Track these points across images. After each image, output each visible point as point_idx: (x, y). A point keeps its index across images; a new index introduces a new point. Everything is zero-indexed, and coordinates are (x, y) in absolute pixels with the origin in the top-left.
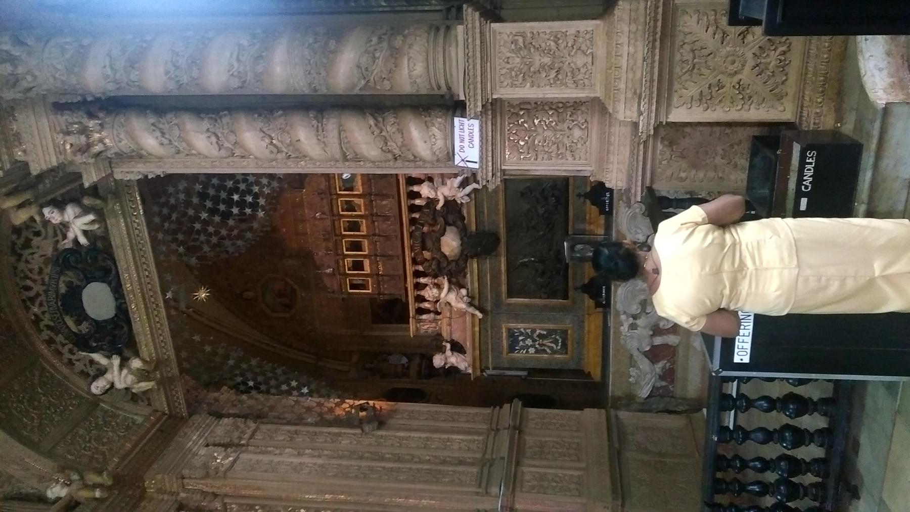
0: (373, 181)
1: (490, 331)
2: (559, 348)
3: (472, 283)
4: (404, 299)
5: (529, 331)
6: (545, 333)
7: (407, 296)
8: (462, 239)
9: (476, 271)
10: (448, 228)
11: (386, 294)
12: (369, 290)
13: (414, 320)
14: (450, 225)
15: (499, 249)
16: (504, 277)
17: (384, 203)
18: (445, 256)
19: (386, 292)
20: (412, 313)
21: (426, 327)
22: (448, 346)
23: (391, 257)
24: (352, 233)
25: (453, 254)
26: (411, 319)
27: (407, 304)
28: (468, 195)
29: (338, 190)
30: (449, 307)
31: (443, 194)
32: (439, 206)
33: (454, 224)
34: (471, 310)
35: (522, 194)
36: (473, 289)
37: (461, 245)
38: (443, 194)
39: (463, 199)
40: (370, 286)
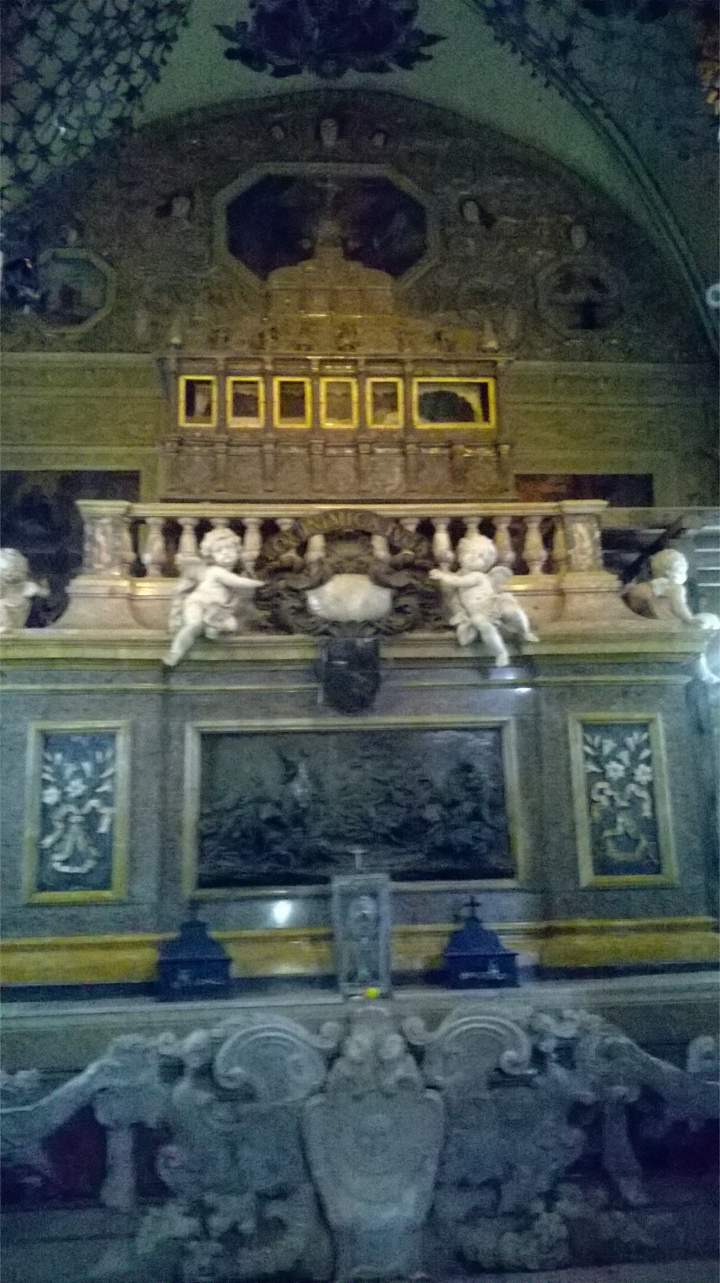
1: (108, 687)
2: (58, 866)
3: (251, 646)
5: (106, 787)
6: (103, 829)
8: (368, 624)
9: (280, 655)
13: (122, 510)
14: (394, 599)
15: (331, 712)
16: (258, 724)
20: (140, 509)
21: (100, 538)
22: (45, 592)
26: (126, 503)
28: (478, 641)
31: (476, 585)
32: (435, 574)
35: (467, 768)
36: (231, 647)
37: (352, 624)
38: (476, 585)
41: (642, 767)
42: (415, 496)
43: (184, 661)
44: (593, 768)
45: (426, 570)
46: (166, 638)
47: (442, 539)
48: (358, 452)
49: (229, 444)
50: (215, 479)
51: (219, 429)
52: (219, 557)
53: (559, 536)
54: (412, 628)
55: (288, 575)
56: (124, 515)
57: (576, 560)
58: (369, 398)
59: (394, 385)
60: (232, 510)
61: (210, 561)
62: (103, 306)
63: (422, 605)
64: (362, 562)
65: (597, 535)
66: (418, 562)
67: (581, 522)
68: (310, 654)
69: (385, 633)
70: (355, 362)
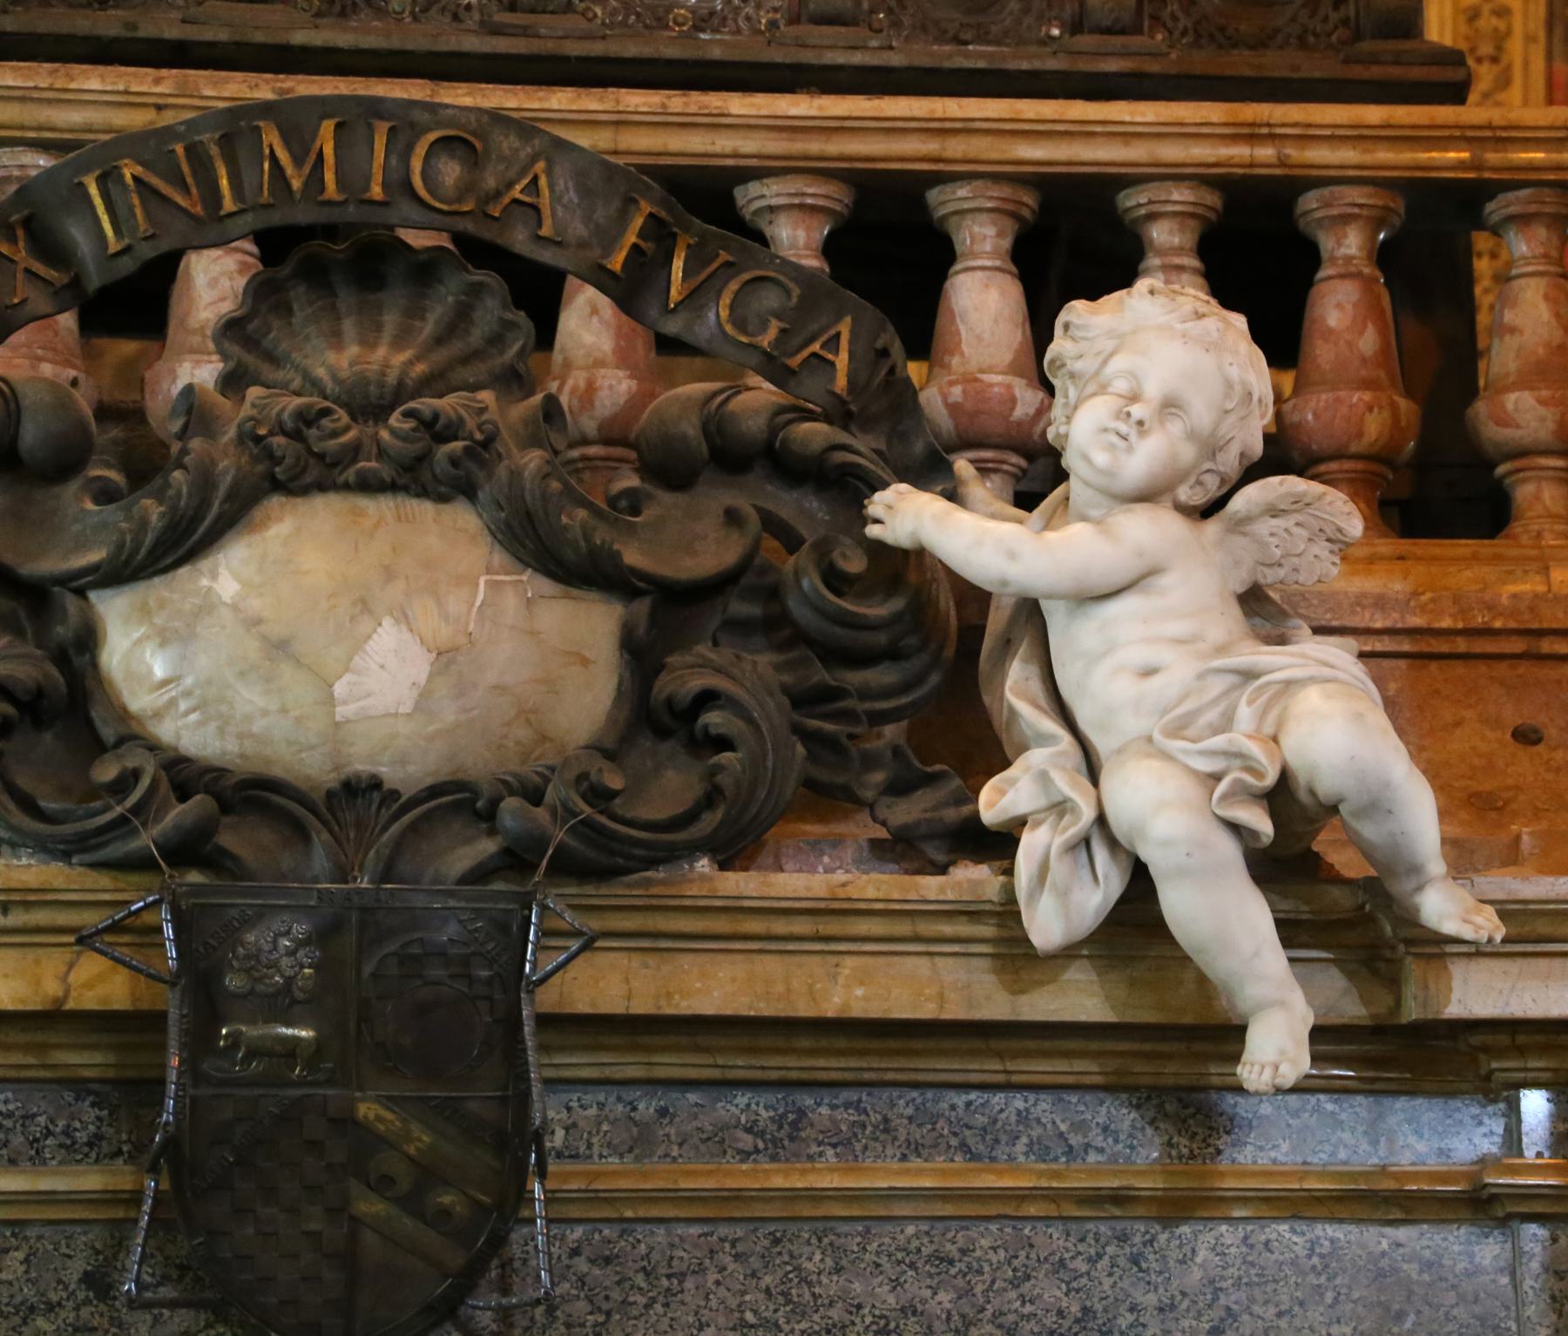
63: (804, 700)
64: (436, 429)
66: (813, 434)
69: (567, 868)
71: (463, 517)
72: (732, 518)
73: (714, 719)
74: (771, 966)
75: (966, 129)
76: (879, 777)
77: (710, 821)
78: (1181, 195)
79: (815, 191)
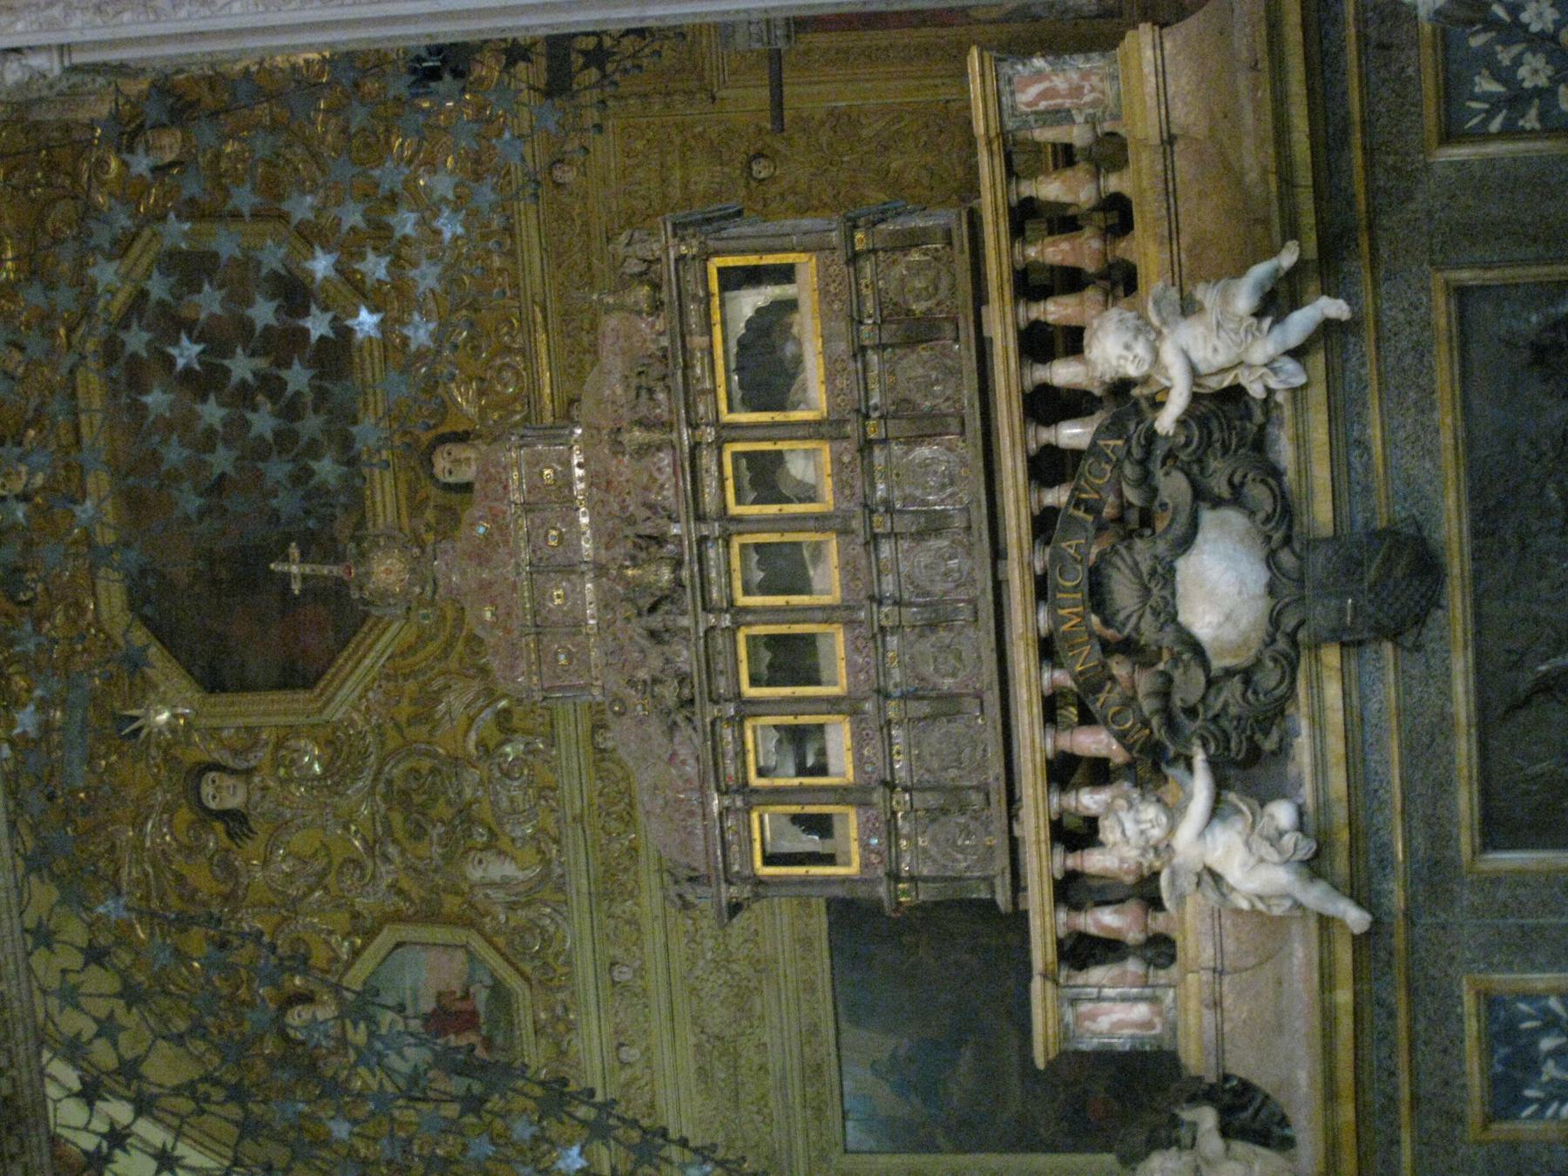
0: (873, 358)
4: (1003, 898)
7: (1017, 884)
8: (1271, 560)
9: (1335, 717)
10: (1208, 517)
11: (926, 880)
12: (848, 864)
13: (1049, 985)
14: (1217, 503)
16: (1464, 748)
17: (924, 452)
18: (1196, 648)
19: (925, 872)
20: (1041, 952)
22: (1207, 1118)
23: (948, 705)
24: (779, 600)
25: (1230, 634)
26: (1037, 984)
27: (1019, 920)
29: (723, 406)
30: (1212, 896)
31: (1186, 354)
32: (1166, 422)
33: (1237, 498)
34: (1316, 896)
36: (1323, 806)
37: (1271, 590)
38: (1186, 354)
39: (1275, 371)
40: (855, 847)
41: (1525, 17)
42: (975, 423)
43: (1360, 895)
44: (1530, 121)
45: (1151, 436)
46: (1313, 924)
47: (1063, 373)
48: (887, 536)
49: (890, 786)
50: (962, 811)
51: (864, 804)
52: (1156, 833)
53: (1047, 134)
54: (1276, 473)
55: (1177, 701)
56: (1056, 983)
57: (1094, 104)
58: (772, 509)
59: (736, 456)
60: (1031, 783)
61: (1162, 846)
62: (465, 947)
64: (1153, 572)
65: (1038, 62)
67: (1012, 93)
68: (1331, 656)
69: (1290, 527)
70: (702, 540)
71: (1180, 564)
72: (1167, 474)
73: (1237, 479)
74: (1314, 457)
75: (1008, 386)
76: (1248, 425)
77: (1272, 482)
78: (1021, 310)
79: (1031, 432)
